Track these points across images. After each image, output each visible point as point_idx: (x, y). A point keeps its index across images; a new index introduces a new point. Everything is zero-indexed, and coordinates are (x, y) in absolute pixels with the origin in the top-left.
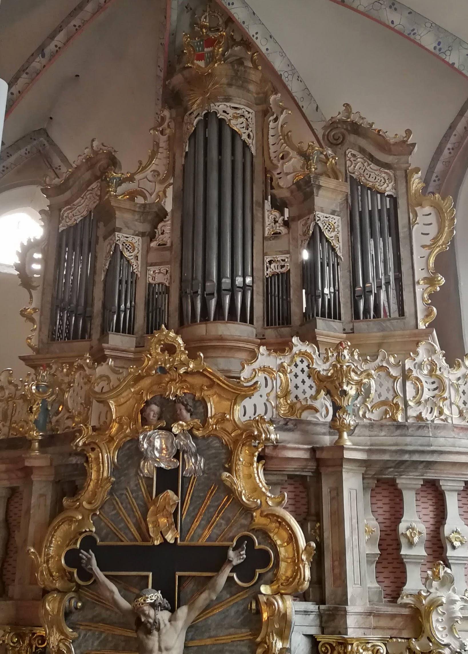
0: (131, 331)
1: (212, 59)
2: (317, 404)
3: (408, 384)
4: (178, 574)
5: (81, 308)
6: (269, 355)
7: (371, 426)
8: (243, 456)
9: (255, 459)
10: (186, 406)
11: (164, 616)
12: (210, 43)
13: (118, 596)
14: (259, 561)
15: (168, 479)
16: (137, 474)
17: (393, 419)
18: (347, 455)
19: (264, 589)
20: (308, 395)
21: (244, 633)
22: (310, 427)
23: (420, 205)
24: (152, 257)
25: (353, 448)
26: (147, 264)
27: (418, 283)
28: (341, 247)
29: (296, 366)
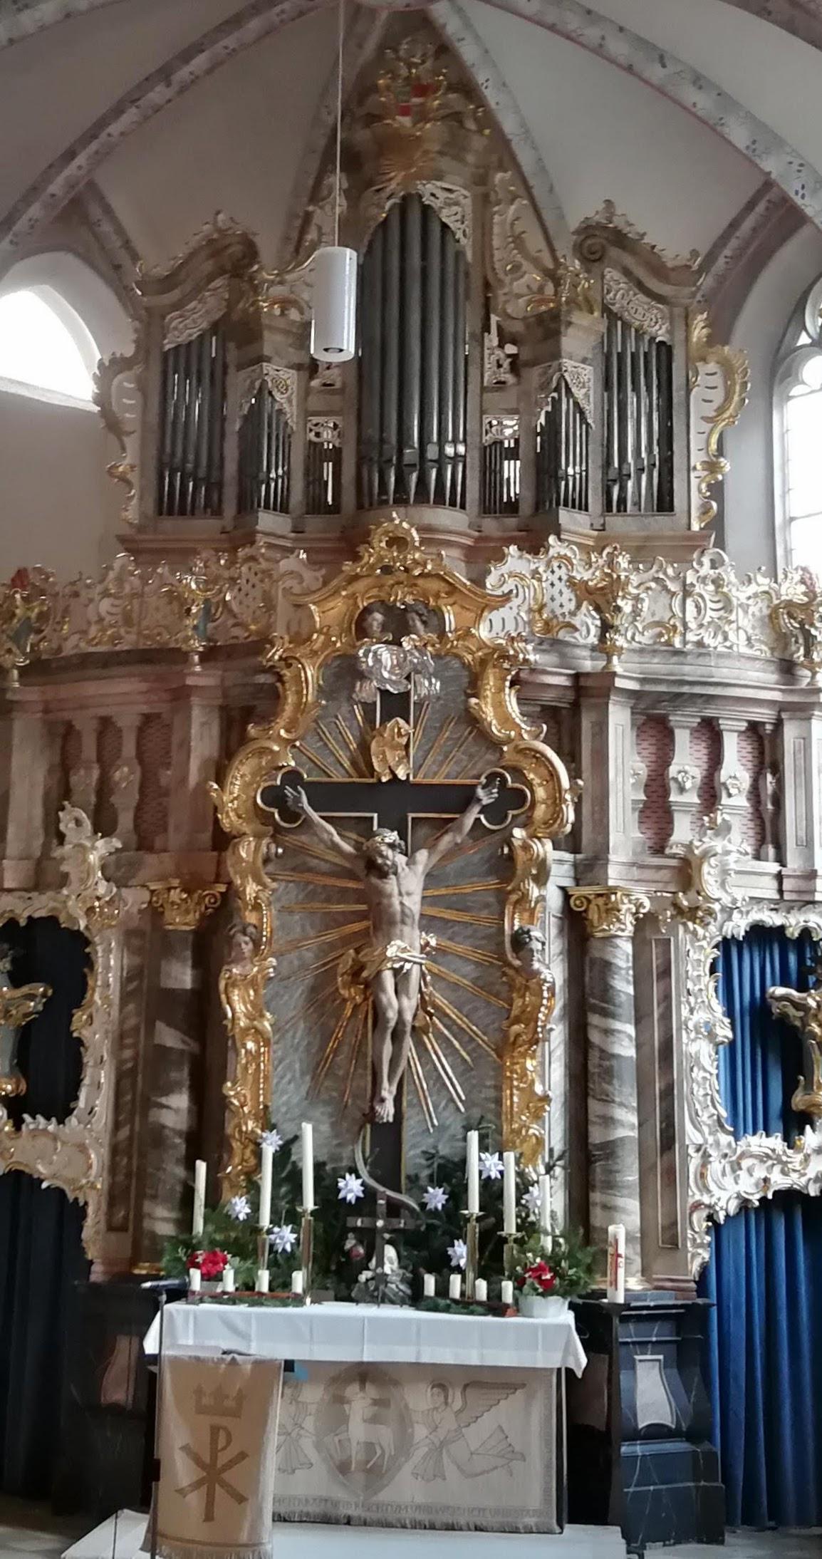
1: (422, 116)
2: (576, 621)
3: (689, 602)
4: (411, 816)
5: (202, 473)
6: (520, 557)
7: (641, 651)
8: (491, 680)
9: (508, 684)
10: (420, 615)
11: (401, 860)
12: (423, 90)
13: (337, 838)
14: (513, 800)
15: (396, 704)
16: (350, 698)
17: (669, 643)
18: (619, 683)
19: (518, 833)
20: (565, 610)
21: (493, 882)
22: (567, 650)
23: (704, 360)
24: (315, 402)
26: (307, 413)
27: (695, 468)
29: (553, 572)
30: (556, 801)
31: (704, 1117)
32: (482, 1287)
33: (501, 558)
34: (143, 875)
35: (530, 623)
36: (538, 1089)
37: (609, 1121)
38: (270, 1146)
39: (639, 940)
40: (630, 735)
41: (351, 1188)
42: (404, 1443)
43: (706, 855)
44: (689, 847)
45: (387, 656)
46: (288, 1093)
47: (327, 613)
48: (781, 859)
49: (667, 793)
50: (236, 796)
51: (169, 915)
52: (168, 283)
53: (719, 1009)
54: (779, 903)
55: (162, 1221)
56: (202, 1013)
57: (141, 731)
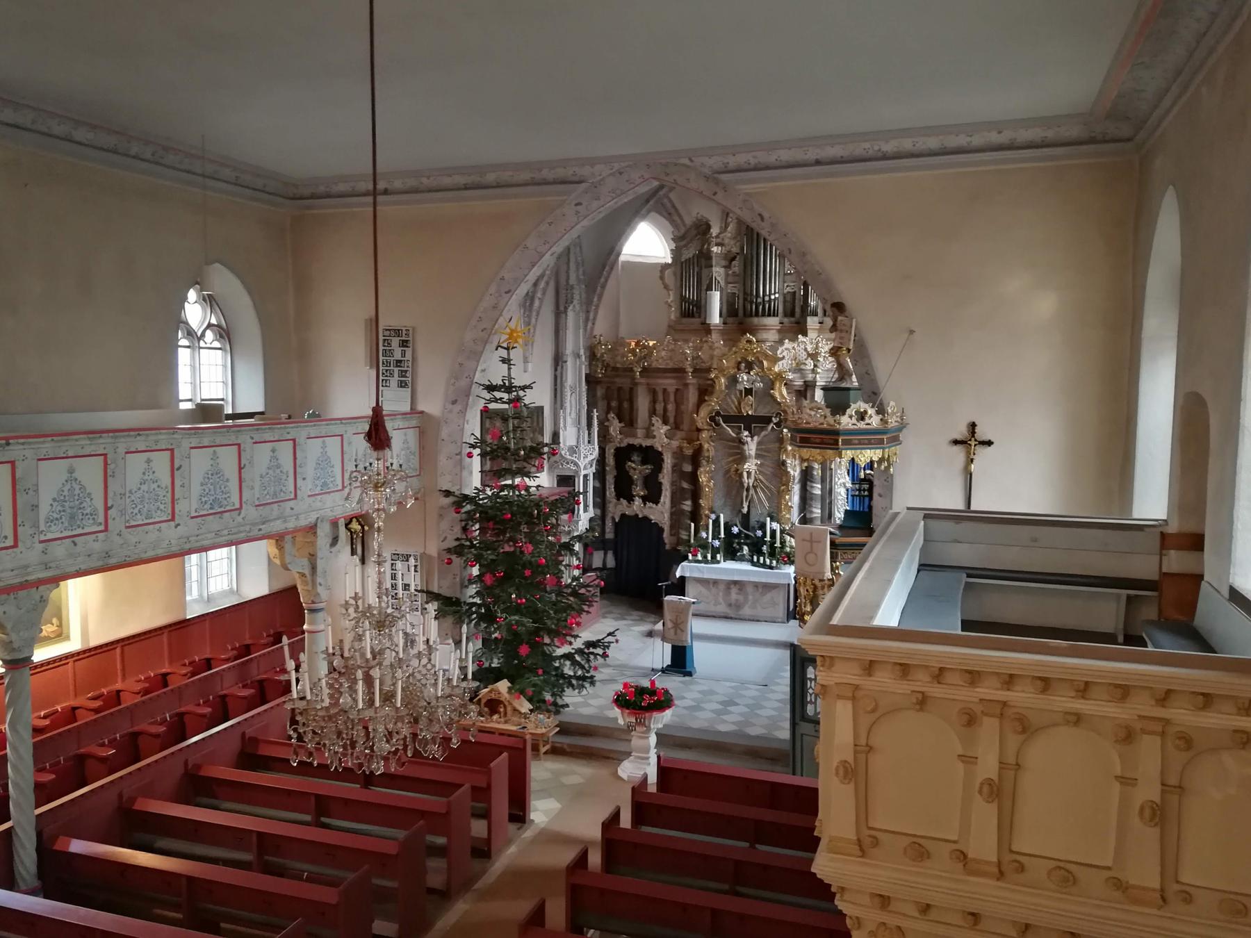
15: (749, 392)
21: (777, 445)
24: (730, 279)
25: (821, 382)
26: (727, 283)
32: (768, 561)
37: (812, 512)
38: (713, 516)
41: (735, 530)
42: (746, 599)
46: (718, 503)
50: (702, 418)
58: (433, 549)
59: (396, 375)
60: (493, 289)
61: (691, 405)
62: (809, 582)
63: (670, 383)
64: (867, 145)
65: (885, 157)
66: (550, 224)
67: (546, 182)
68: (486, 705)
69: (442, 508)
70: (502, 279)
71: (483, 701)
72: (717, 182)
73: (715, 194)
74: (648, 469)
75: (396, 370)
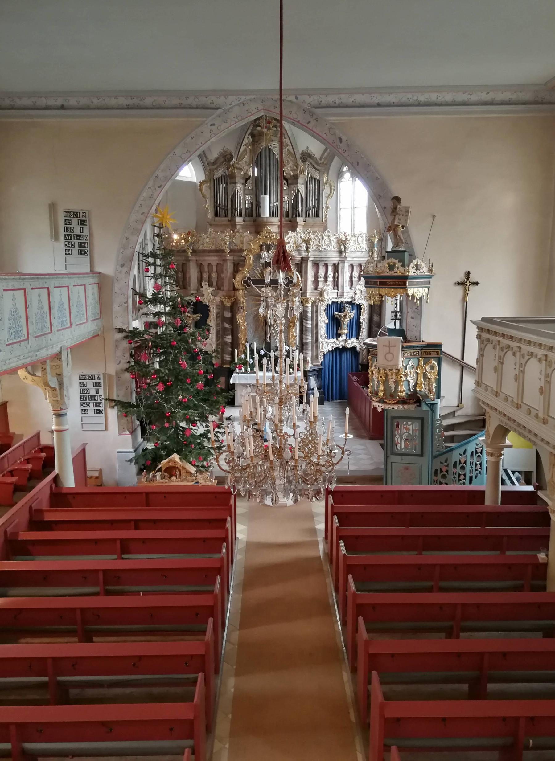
0: (241, 216)
2: (302, 245)
24: (247, 192)
26: (245, 195)
28: (303, 195)
30: (298, 281)
31: (323, 336)
33: (288, 233)
34: (219, 295)
35: (293, 247)
36: (295, 334)
37: (307, 339)
39: (312, 306)
40: (312, 267)
43: (325, 290)
44: (322, 289)
45: (266, 255)
46: (250, 337)
47: (254, 246)
48: (338, 289)
49: (318, 278)
50: (238, 281)
51: (225, 303)
52: (214, 163)
53: (326, 317)
54: (336, 298)
55: (228, 358)
56: (232, 321)
57: (216, 267)
58: (112, 370)
59: (76, 245)
60: (150, 183)
61: (229, 274)
62: (382, 372)
63: (213, 260)
64: (410, 96)
65: (419, 104)
66: (192, 138)
67: (191, 108)
68: (165, 471)
69: (117, 341)
70: (157, 177)
71: (163, 469)
72: (312, 114)
73: (309, 122)
74: (198, 317)
75: (77, 242)
